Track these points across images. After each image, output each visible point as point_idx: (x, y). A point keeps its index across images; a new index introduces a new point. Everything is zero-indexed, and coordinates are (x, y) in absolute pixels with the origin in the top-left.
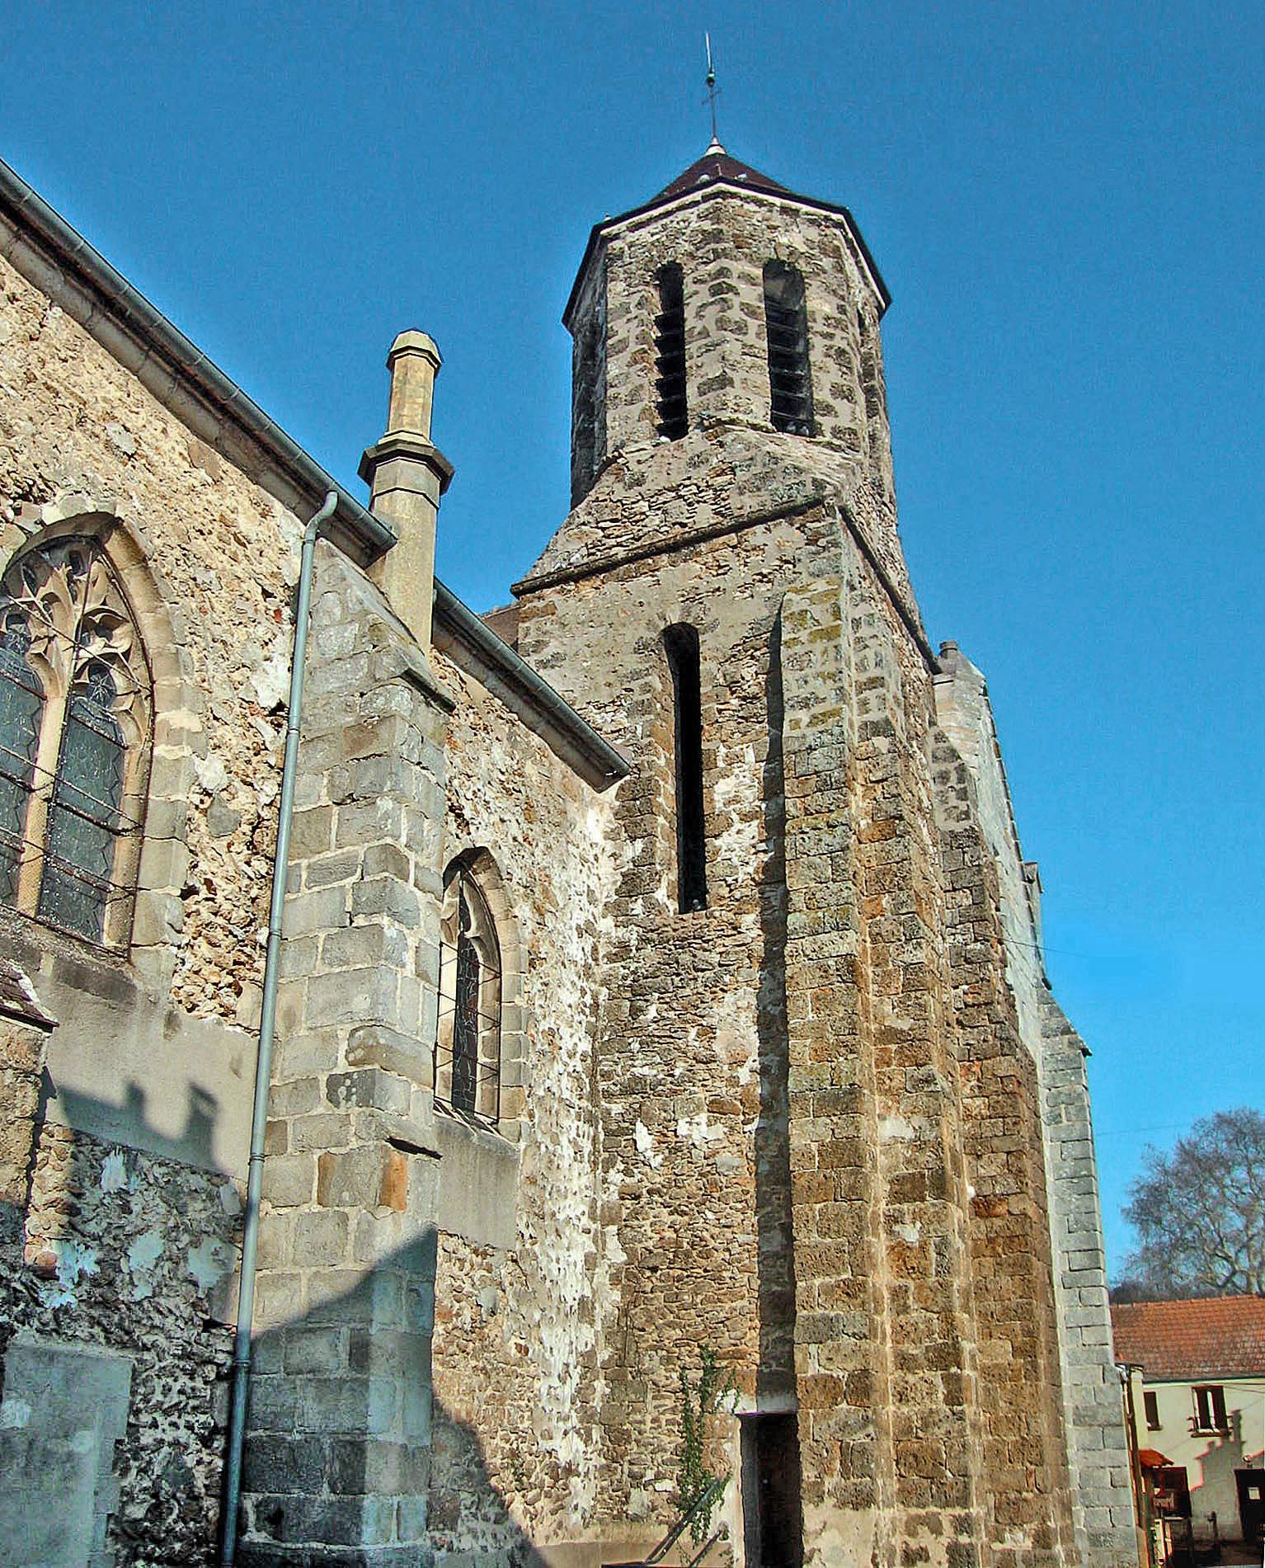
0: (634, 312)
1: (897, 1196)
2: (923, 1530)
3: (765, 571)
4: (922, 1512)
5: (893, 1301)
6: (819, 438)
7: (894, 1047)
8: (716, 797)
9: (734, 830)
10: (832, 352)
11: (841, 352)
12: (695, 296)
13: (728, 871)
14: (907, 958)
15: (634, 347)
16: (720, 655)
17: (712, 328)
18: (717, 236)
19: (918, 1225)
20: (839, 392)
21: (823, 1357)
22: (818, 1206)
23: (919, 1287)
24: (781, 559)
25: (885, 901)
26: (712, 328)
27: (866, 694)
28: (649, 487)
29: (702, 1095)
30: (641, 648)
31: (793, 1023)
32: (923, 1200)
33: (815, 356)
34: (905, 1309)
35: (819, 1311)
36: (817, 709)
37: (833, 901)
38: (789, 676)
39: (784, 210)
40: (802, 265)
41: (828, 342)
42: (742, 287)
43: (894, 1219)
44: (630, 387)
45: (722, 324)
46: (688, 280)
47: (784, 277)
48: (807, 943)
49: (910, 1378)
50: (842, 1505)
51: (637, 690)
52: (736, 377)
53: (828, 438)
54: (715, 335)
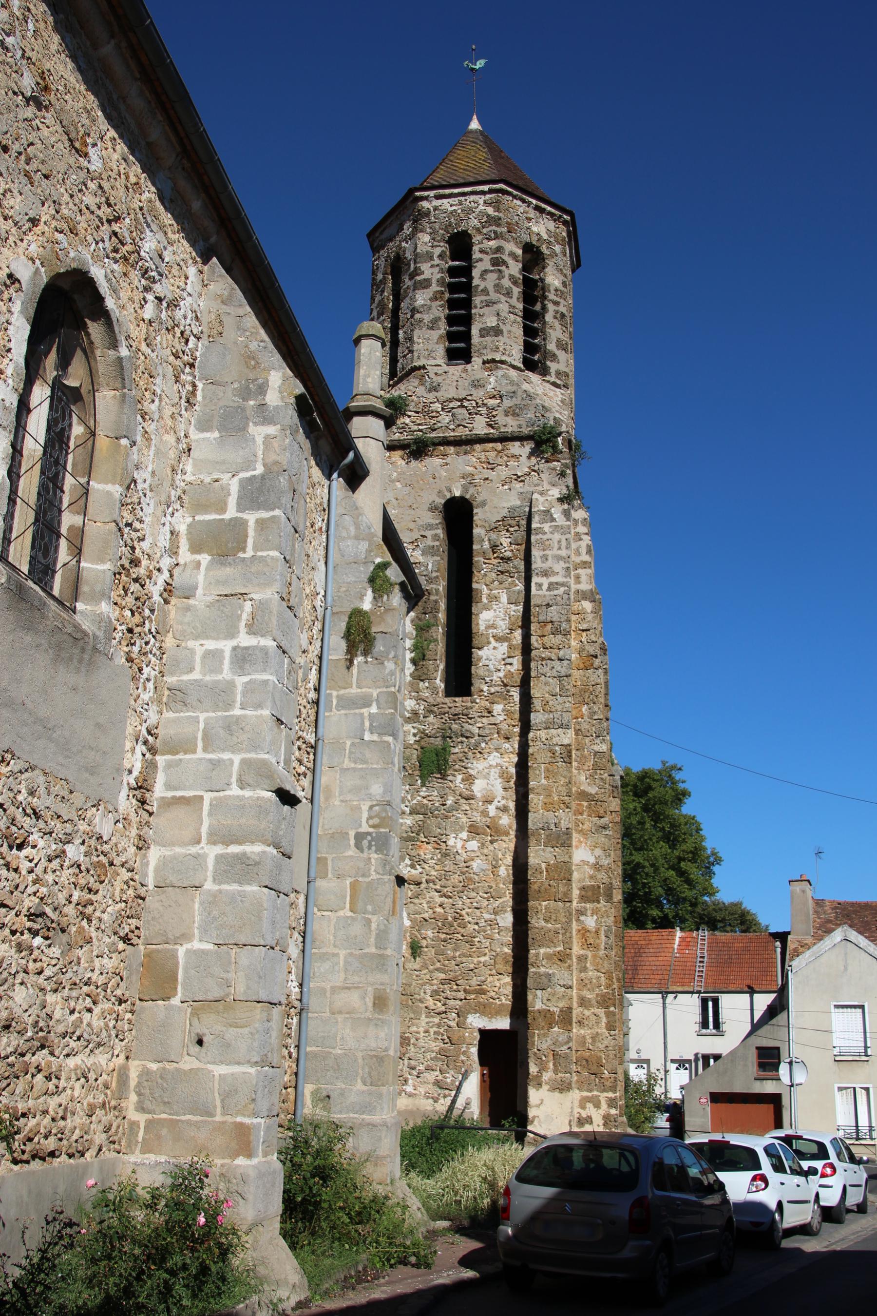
0: (437, 261)
1: (583, 898)
2: (589, 1105)
3: (519, 474)
4: (589, 1094)
5: (578, 964)
6: (548, 378)
7: (585, 804)
8: (481, 622)
9: (491, 646)
10: (558, 316)
11: (563, 316)
12: (481, 264)
13: (487, 673)
14: (596, 748)
15: (435, 287)
16: (487, 525)
17: (491, 289)
18: (497, 221)
19: (595, 917)
20: (561, 345)
21: (545, 999)
22: (544, 903)
23: (594, 956)
24: (529, 467)
25: (585, 709)
26: (491, 289)
27: (579, 571)
28: (443, 394)
29: (464, 819)
30: (433, 508)
31: (532, 784)
32: (599, 902)
33: (549, 317)
34: (584, 969)
35: (543, 970)
36: (553, 579)
37: (559, 708)
38: (536, 553)
39: (537, 208)
40: (544, 249)
41: (556, 308)
42: (510, 262)
43: (581, 912)
44: (432, 317)
45: (498, 287)
46: (476, 248)
47: (533, 256)
48: (543, 734)
49: (587, 1013)
50: (553, 1089)
51: (429, 537)
52: (505, 329)
53: (553, 379)
54: (493, 296)
